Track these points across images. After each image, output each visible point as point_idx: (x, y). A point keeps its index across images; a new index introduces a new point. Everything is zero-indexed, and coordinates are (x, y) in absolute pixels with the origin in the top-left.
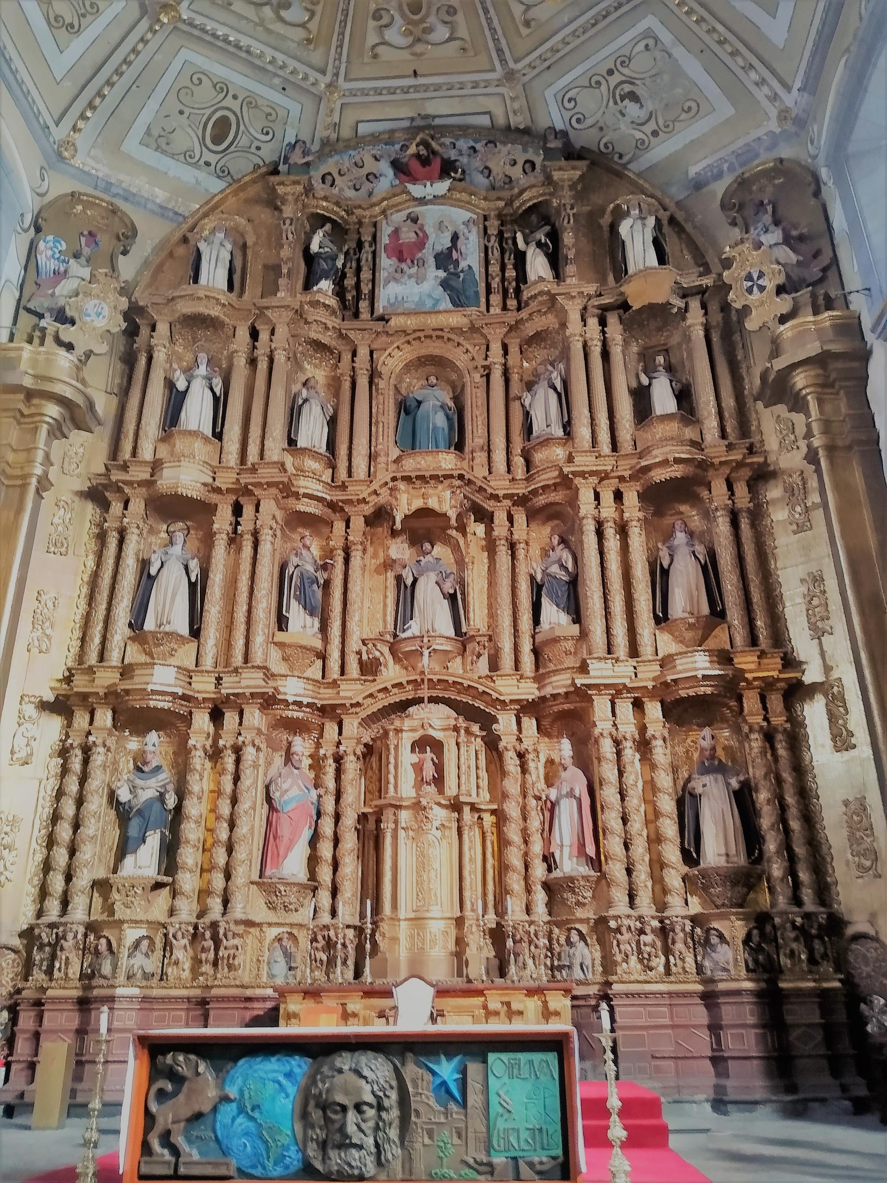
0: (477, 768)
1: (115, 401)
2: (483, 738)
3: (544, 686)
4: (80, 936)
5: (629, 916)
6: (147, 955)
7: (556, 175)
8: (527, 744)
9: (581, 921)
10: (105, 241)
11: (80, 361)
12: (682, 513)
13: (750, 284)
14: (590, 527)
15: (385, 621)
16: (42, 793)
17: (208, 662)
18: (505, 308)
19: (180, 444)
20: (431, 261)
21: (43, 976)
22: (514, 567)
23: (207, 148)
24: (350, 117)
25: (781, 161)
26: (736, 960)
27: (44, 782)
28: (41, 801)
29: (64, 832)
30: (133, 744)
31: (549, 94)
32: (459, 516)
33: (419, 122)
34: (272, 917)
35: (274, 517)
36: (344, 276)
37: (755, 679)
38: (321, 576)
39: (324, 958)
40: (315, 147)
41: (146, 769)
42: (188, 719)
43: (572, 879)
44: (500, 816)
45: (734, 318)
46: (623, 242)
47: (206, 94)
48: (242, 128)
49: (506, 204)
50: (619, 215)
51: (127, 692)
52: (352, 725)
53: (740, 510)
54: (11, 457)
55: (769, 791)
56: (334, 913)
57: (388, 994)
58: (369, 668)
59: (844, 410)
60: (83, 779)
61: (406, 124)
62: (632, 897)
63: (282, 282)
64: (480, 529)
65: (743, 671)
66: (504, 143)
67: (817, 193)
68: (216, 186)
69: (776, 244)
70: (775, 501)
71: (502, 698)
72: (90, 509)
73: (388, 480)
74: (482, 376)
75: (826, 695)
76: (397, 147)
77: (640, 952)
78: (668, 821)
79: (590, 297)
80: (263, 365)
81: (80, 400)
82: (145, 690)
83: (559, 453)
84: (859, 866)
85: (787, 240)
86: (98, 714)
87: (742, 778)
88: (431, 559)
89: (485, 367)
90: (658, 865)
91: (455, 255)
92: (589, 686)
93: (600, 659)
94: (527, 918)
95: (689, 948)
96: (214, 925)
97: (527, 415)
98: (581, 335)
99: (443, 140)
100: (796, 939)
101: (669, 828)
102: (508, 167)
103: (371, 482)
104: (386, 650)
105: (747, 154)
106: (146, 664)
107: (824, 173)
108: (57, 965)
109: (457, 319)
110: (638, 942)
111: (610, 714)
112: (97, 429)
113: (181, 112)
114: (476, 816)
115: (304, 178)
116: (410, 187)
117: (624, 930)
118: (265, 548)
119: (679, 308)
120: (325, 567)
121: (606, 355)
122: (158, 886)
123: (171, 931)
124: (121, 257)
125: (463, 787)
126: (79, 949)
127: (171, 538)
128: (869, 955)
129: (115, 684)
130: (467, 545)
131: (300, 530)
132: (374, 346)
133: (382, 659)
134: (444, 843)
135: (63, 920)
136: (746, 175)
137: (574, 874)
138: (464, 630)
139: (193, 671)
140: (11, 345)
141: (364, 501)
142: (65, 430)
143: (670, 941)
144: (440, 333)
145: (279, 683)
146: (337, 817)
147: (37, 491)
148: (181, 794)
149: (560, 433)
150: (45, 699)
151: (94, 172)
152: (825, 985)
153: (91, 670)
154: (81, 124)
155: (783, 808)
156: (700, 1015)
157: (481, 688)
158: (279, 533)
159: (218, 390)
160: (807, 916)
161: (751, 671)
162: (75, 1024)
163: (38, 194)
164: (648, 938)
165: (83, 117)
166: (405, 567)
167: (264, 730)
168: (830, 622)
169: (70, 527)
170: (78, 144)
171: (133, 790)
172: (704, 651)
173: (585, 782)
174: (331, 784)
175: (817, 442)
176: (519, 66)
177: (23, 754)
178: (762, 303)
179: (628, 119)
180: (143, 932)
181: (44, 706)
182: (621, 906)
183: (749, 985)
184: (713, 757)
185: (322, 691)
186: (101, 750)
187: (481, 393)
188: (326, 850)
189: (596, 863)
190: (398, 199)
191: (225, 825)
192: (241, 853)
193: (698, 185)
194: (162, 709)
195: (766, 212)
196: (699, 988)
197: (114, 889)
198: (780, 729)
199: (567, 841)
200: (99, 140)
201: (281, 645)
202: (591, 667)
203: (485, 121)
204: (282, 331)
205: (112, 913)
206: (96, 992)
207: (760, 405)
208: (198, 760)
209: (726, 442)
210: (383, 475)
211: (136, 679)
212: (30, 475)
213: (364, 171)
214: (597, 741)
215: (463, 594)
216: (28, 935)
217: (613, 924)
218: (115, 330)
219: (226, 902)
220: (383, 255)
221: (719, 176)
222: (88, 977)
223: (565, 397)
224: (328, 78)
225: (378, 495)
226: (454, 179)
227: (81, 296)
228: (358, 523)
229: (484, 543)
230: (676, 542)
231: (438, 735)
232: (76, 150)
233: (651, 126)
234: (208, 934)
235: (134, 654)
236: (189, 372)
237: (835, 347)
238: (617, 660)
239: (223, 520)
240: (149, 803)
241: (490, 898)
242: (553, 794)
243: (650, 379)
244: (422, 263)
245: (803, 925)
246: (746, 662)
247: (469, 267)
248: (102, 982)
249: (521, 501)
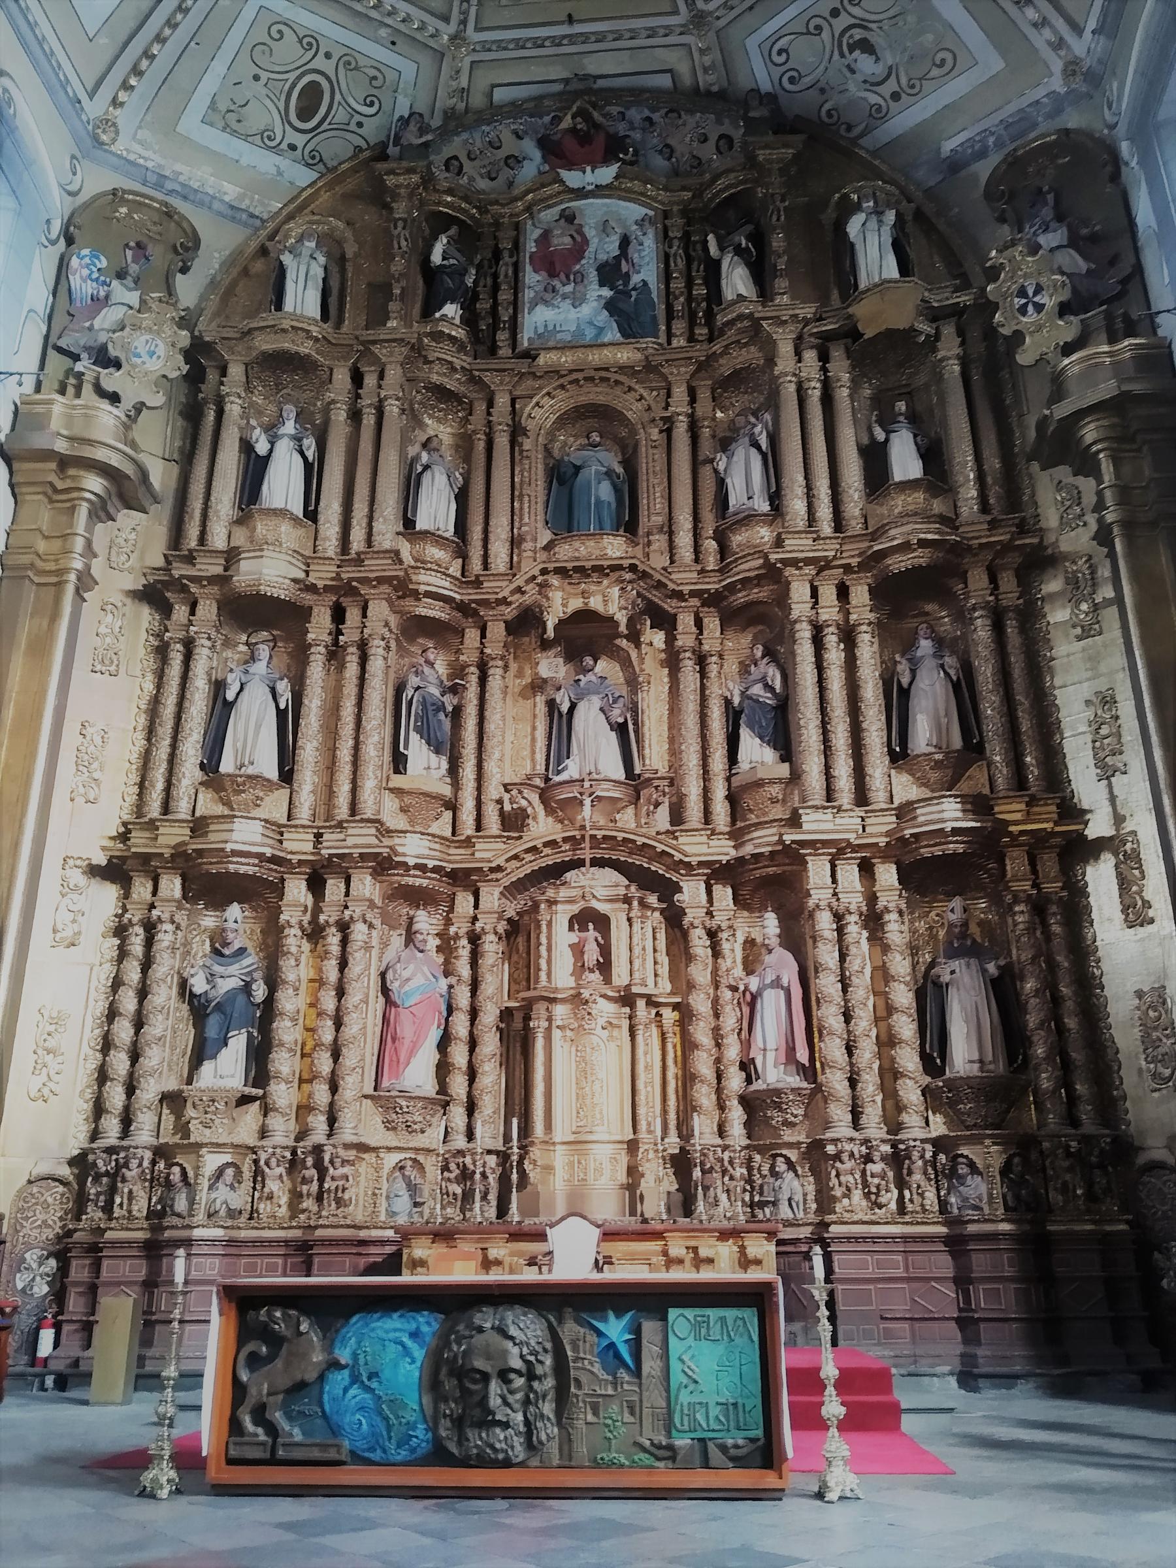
0: (655, 951)
1: (175, 470)
2: (662, 911)
3: (742, 844)
4: (146, 1164)
5: (852, 1139)
6: (232, 1187)
7: (762, 155)
8: (720, 919)
9: (790, 1145)
10: (158, 254)
11: (128, 416)
12: (927, 614)
13: (1024, 301)
14: (804, 633)
15: (533, 760)
16: (94, 983)
17: (304, 814)
18: (691, 339)
19: (262, 527)
20: (593, 275)
21: (100, 1214)
22: (703, 688)
23: (290, 123)
24: (484, 79)
25: (1067, 132)
26: (990, 1195)
27: (96, 969)
28: (93, 994)
29: (123, 1031)
30: (209, 920)
31: (752, 43)
32: (630, 620)
33: (575, 86)
34: (391, 1139)
35: (387, 625)
36: (475, 297)
37: (1022, 833)
38: (449, 701)
39: (459, 1191)
40: (436, 122)
41: (226, 952)
42: (279, 889)
43: (778, 1092)
44: (685, 1013)
45: (1002, 349)
46: (852, 245)
47: (289, 52)
48: (338, 97)
49: (693, 197)
50: (848, 209)
51: (200, 853)
52: (491, 897)
53: (1007, 609)
54: (42, 546)
55: (1037, 978)
56: (470, 1135)
57: (541, 1236)
58: (514, 822)
59: (1147, 472)
60: (147, 965)
61: (558, 87)
62: (856, 1114)
63: (393, 306)
64: (658, 638)
65: (1008, 823)
66: (691, 112)
67: (1116, 176)
68: (304, 177)
69: (1058, 247)
70: (1052, 597)
71: (687, 859)
72: (146, 616)
73: (536, 572)
74: (661, 432)
75: (1116, 855)
76: (547, 119)
77: (865, 1184)
78: (904, 1018)
79: (806, 322)
80: (369, 420)
81: (128, 469)
82: (223, 850)
83: (764, 534)
84: (1155, 1076)
85: (1073, 242)
86: (164, 882)
87: (1002, 962)
88: (593, 678)
89: (665, 420)
90: (890, 1075)
91: (624, 267)
92: (803, 844)
93: (816, 807)
94: (719, 1141)
95: (929, 1180)
96: (318, 1150)
97: (721, 483)
98: (795, 375)
99: (608, 108)
100: (1070, 1169)
101: (906, 1027)
102: (695, 144)
103: (514, 575)
104: (535, 798)
105: (1022, 123)
106: (223, 817)
107: (1125, 147)
108: (118, 1200)
109: (625, 355)
110: (864, 1172)
111: (830, 880)
112: (153, 508)
113: (256, 78)
114: (654, 1012)
115: (423, 163)
116: (565, 174)
117: (845, 1157)
118: (376, 665)
119: (928, 336)
120: (454, 690)
121: (827, 400)
122: (244, 1100)
123: (263, 1157)
124: (179, 275)
125: (636, 975)
126: (145, 1180)
127: (252, 652)
128: (1166, 1190)
129: (183, 843)
130: (642, 660)
131: (420, 641)
132: (517, 393)
133: (529, 810)
134: (612, 1046)
135: (125, 1143)
136: (1020, 152)
137: (780, 1085)
138: (637, 771)
139: (285, 826)
140: (38, 397)
141: (504, 602)
142: (112, 510)
143: (905, 1171)
144: (604, 374)
145: (397, 841)
146: (474, 1013)
147: (77, 590)
148: (273, 983)
149: (765, 507)
150: (94, 862)
151: (141, 161)
152: (1108, 1228)
153: (152, 825)
154: (123, 96)
155: (1056, 1001)
156: (943, 1264)
157: (660, 847)
158: (393, 644)
159: (310, 454)
160: (1086, 1140)
161: (1016, 823)
162: (142, 1274)
163: (70, 194)
164: (876, 1167)
165: (126, 86)
166: (559, 689)
167: (378, 901)
168: (1124, 757)
169: (121, 639)
170: (119, 122)
171: (211, 978)
172: (956, 796)
173: (795, 967)
174: (465, 971)
175: (1110, 517)
176: (711, 7)
177: (68, 933)
178: (1039, 328)
179: (859, 77)
180: (228, 1158)
181: (94, 871)
182: (842, 1127)
183: (1005, 1227)
184: (964, 935)
185: (452, 851)
186: (169, 927)
187: (660, 455)
188: (459, 1055)
189: (809, 1072)
190: (547, 191)
191: (330, 1023)
192: (350, 1058)
193: (955, 165)
194: (245, 875)
195: (1046, 204)
196: (943, 1230)
197: (189, 1104)
198: (1054, 897)
199: (771, 1045)
200: (148, 118)
201: (398, 792)
202: (804, 818)
203: (665, 81)
204: (394, 374)
205: (186, 1134)
206: (167, 1234)
207: (1035, 466)
208: (294, 940)
209: (989, 518)
210: (530, 567)
211: (212, 837)
212: (66, 570)
213: (501, 154)
214: (811, 915)
215: (636, 724)
216: (80, 1162)
217: (830, 1149)
218: (174, 374)
219: (332, 1120)
220: (528, 268)
221: (982, 154)
222: (156, 1216)
224: (452, 28)
225: (523, 593)
226: (624, 162)
227: (127, 329)
228: (497, 631)
229: (663, 656)
230: (919, 653)
231: (602, 907)
232: (117, 133)
233: (891, 86)
234: (310, 1161)
235: (208, 804)
236: (272, 430)
237: (1136, 387)
238: (839, 809)
239: (319, 627)
240: (231, 994)
241: (672, 1116)
242: (754, 983)
243: (888, 432)
244: (580, 278)
245: (1079, 1150)
246: (1011, 811)
247: (645, 283)
248: (175, 1221)
249: (712, 600)
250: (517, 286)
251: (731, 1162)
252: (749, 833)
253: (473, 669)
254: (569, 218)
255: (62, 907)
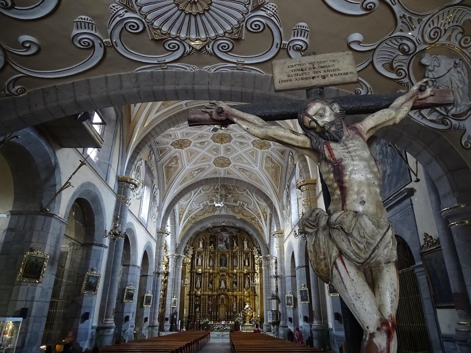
40: (212, 227)
72: (190, 273)
181: (188, 295)
204: (208, 252)
223: (237, 261)
235: (195, 290)
239: (203, 275)
244: (223, 242)
246: (251, 293)
250: (218, 242)
254: (222, 236)
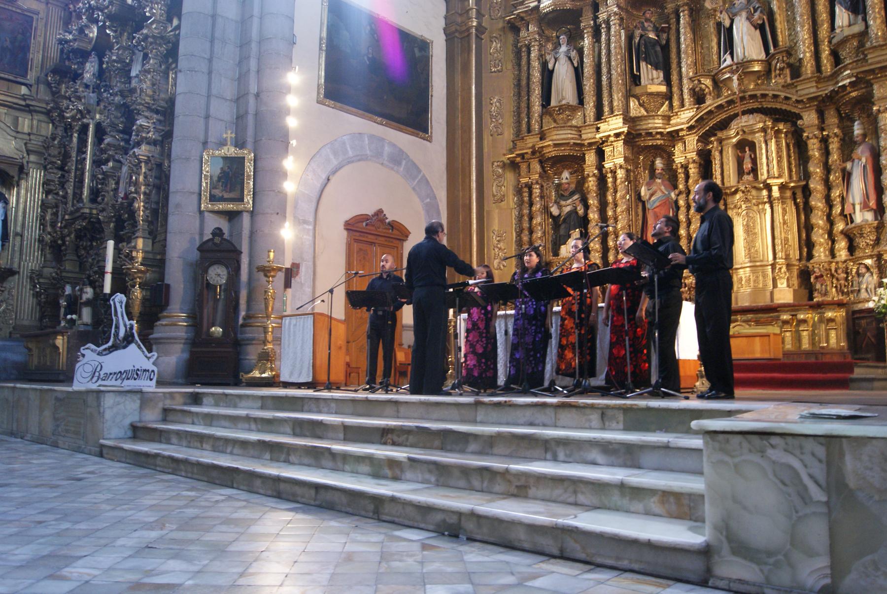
41: (566, 194)
42: (583, 159)
54: (459, 20)
60: (531, 204)
71: (800, 99)
72: (511, 38)
139: (581, 127)
147: (477, 36)
148: (587, 207)
157: (783, 95)
171: (560, 207)
231: (750, 138)
251: (836, 271)
252: (842, 73)
253: (672, 16)
255: (495, 184)
